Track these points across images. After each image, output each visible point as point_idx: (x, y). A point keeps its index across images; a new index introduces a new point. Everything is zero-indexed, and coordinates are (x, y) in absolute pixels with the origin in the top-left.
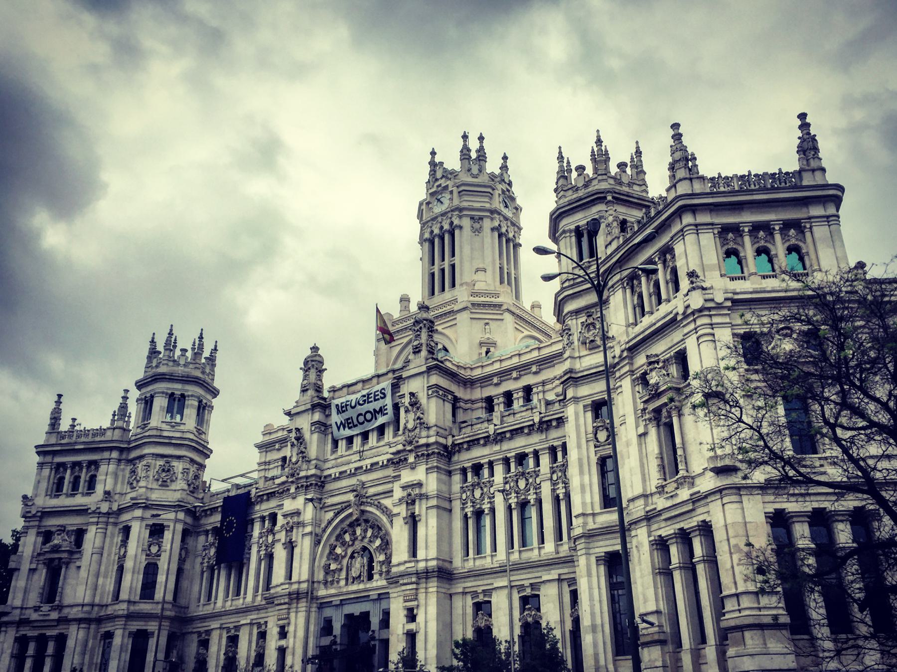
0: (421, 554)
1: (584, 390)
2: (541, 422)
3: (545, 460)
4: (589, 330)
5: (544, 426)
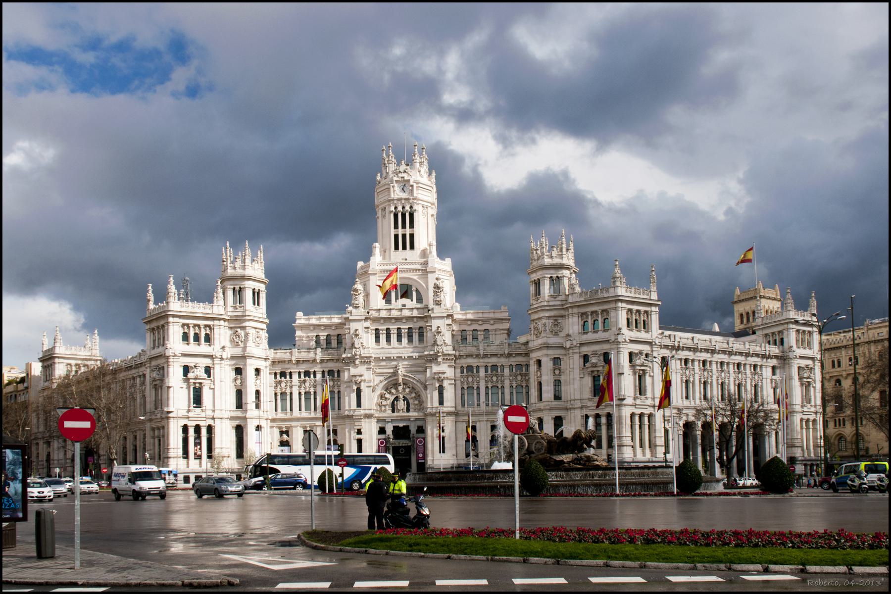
0: (445, 404)
1: (550, 352)
2: (508, 354)
3: (507, 371)
4: (555, 327)
5: (510, 355)
